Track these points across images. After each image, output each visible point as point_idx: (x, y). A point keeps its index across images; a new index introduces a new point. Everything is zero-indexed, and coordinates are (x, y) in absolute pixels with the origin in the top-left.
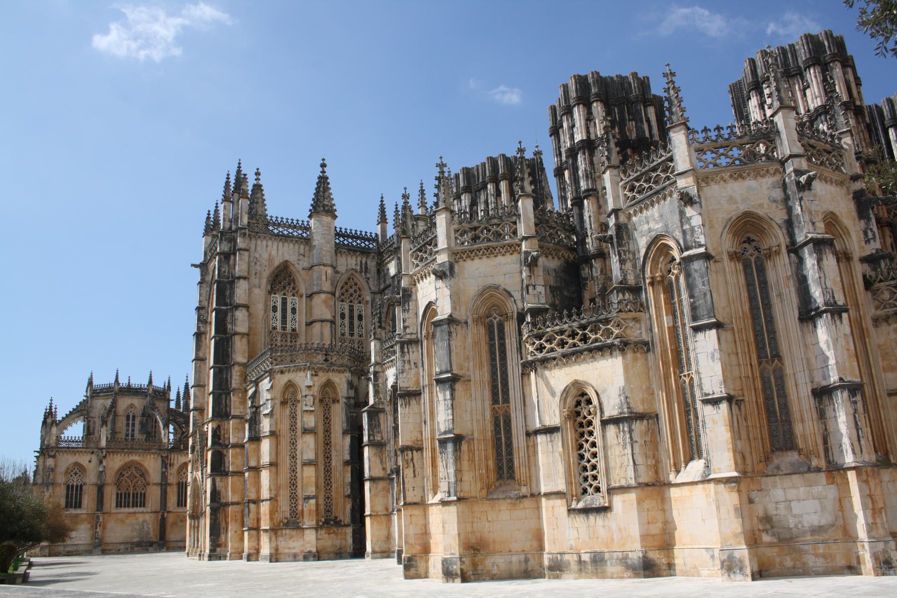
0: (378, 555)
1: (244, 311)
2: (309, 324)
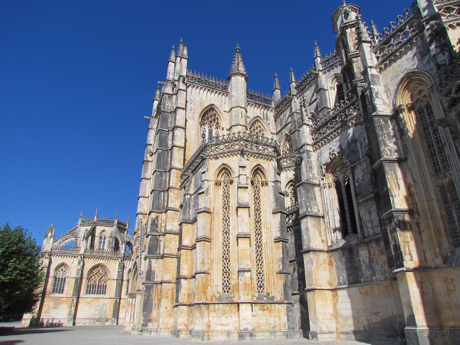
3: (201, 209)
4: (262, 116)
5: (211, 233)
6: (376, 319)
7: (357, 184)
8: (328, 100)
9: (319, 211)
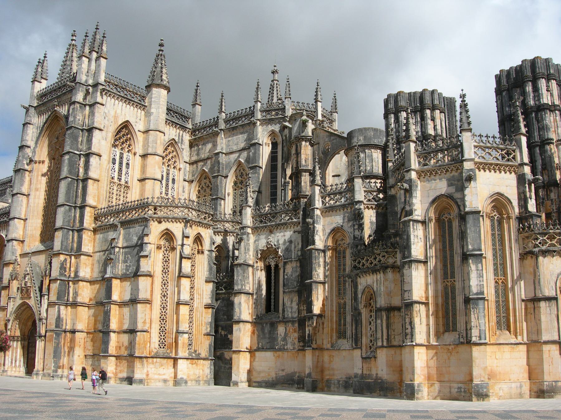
1: (97, 157)
4: (177, 139)
5: (152, 295)
6: (282, 374)
7: (286, 277)
8: (261, 156)
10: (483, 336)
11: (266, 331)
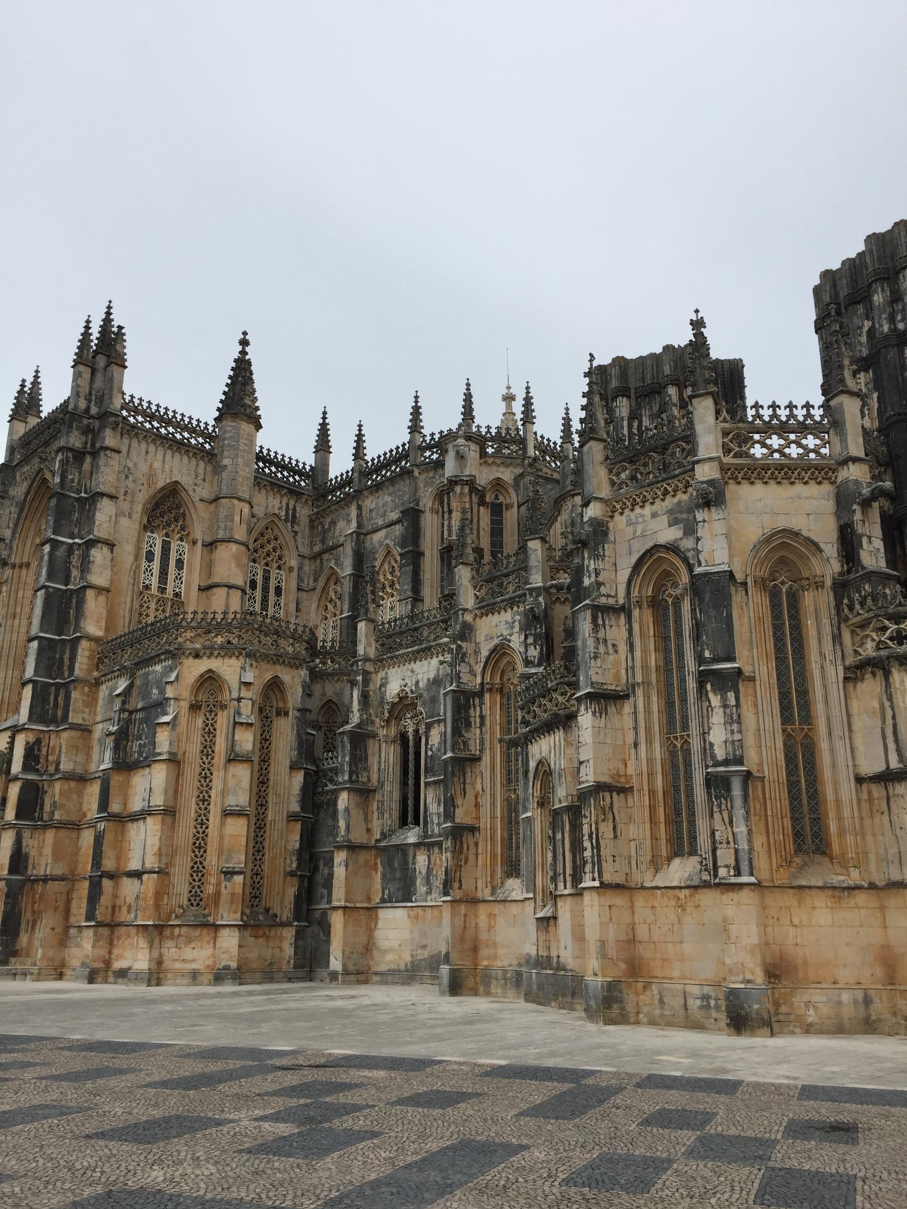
0: (353, 978)
1: (106, 549)
2: (205, 589)
3: (160, 754)
5: (176, 799)
7: (430, 753)
9: (369, 780)
10: (745, 866)
11: (396, 865)
